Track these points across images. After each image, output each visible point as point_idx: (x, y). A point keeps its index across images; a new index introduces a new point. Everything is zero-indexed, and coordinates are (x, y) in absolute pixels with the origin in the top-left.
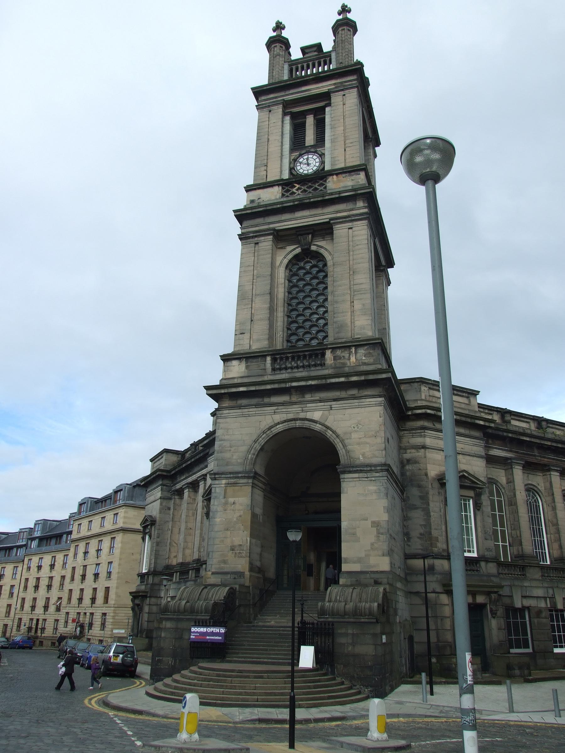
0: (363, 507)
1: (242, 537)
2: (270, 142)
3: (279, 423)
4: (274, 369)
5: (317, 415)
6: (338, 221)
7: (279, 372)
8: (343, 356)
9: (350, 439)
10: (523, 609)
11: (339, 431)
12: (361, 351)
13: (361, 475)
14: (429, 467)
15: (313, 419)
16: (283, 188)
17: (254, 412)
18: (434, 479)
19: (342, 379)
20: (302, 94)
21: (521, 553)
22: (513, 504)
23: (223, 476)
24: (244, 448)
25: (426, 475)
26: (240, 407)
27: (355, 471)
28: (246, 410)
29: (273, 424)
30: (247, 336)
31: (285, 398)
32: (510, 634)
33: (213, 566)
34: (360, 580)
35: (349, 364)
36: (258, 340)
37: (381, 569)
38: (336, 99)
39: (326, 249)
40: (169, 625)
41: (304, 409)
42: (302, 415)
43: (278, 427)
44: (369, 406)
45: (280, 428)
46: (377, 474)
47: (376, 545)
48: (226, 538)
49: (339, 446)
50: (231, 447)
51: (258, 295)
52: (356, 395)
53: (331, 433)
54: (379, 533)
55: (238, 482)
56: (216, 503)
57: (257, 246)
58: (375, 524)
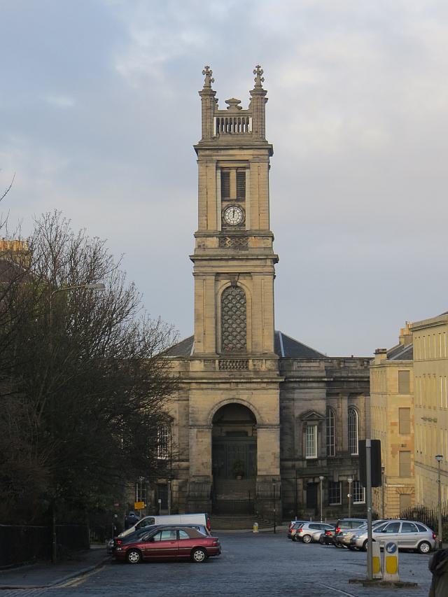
0: (268, 446)
1: (208, 458)
2: (208, 196)
5: (245, 397)
10: (339, 482)
14: (295, 411)
18: (297, 418)
19: (259, 380)
24: (207, 412)
25: (294, 416)
26: (202, 389)
30: (202, 344)
31: (227, 386)
32: (330, 496)
34: (268, 480)
38: (254, 166)
40: (192, 503)
49: (256, 414)
58: (274, 454)
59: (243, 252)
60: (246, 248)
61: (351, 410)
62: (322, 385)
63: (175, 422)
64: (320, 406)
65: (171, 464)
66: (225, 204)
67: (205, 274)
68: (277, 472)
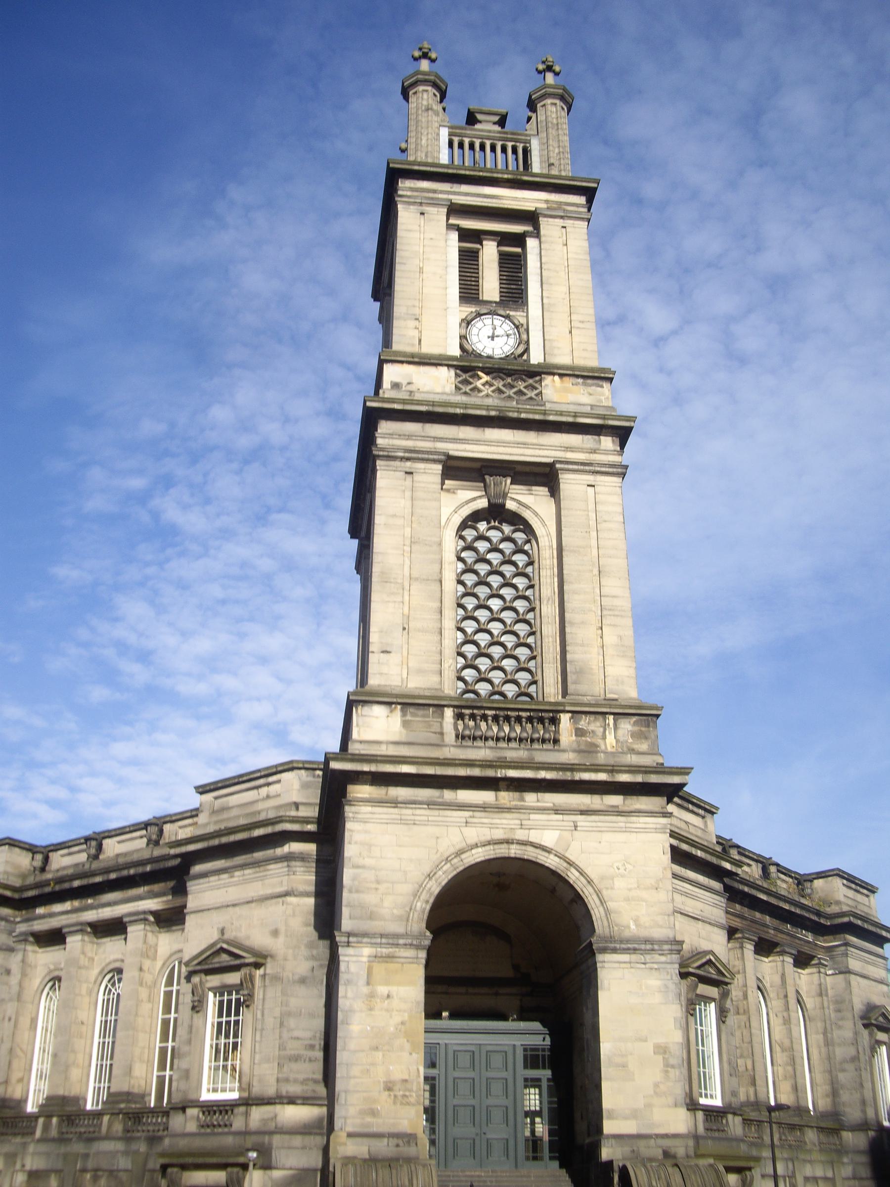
3: (476, 846)
4: (457, 736)
5: (548, 838)
6: (571, 467)
7: (470, 743)
8: (593, 731)
9: (612, 888)
11: (588, 871)
12: (627, 726)
13: (634, 957)
15: (543, 843)
16: (457, 375)
17: (426, 818)
19: (602, 777)
20: (485, 200)
21: (752, 1098)
22: (741, 1011)
23: (365, 940)
24: (407, 888)
26: (395, 803)
27: (624, 949)
28: (409, 812)
29: (464, 845)
30: (394, 659)
33: (348, 1121)
35: (603, 747)
36: (420, 671)
37: (672, 1130)
39: (536, 514)
41: (524, 822)
42: (520, 835)
43: (474, 851)
44: (645, 830)
45: (479, 855)
46: (663, 959)
47: (662, 1087)
48: (373, 1064)
49: (592, 901)
50: (378, 882)
51: (417, 579)
52: (621, 808)
53: (577, 874)
54: (667, 1065)
55: (397, 954)
56: (350, 994)
57: (409, 477)
58: (662, 1050)
62: (717, 885)
63: (270, 968)
65: (247, 1114)
66: (470, 309)
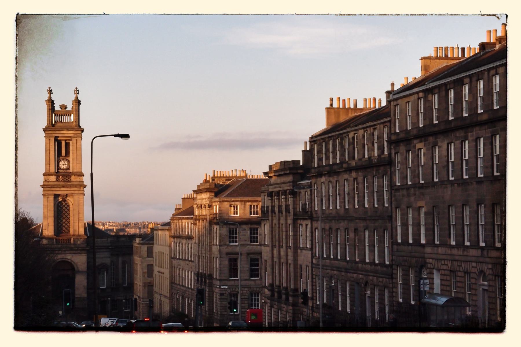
0: (81, 281)
5: (69, 257)
38: (74, 140)
59: (69, 183)
60: (71, 182)
61: (124, 263)
64: (108, 261)
67: (49, 194)
68: (85, 295)
